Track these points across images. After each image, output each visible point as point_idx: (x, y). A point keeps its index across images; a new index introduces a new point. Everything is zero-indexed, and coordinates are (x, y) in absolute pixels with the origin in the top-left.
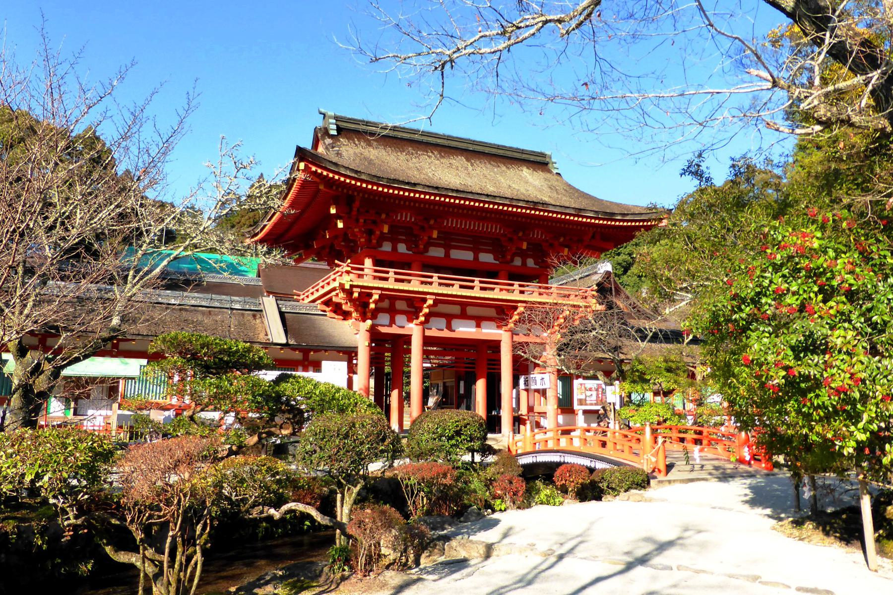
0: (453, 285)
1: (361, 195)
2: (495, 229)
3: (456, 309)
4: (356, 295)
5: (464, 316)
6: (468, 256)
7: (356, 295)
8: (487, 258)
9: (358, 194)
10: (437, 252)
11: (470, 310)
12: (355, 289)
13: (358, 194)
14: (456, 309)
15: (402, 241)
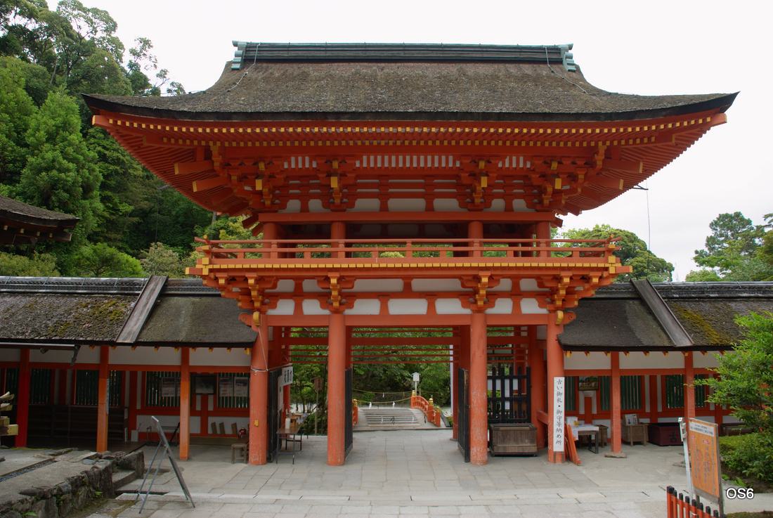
0: (405, 243)
1: (219, 144)
2: (447, 162)
3: (397, 285)
4: (222, 281)
5: (407, 293)
6: (419, 204)
7: (222, 281)
8: (447, 205)
9: (215, 144)
10: (366, 205)
11: (417, 285)
12: (218, 275)
13: (215, 144)
14: (397, 285)
15: (315, 196)
